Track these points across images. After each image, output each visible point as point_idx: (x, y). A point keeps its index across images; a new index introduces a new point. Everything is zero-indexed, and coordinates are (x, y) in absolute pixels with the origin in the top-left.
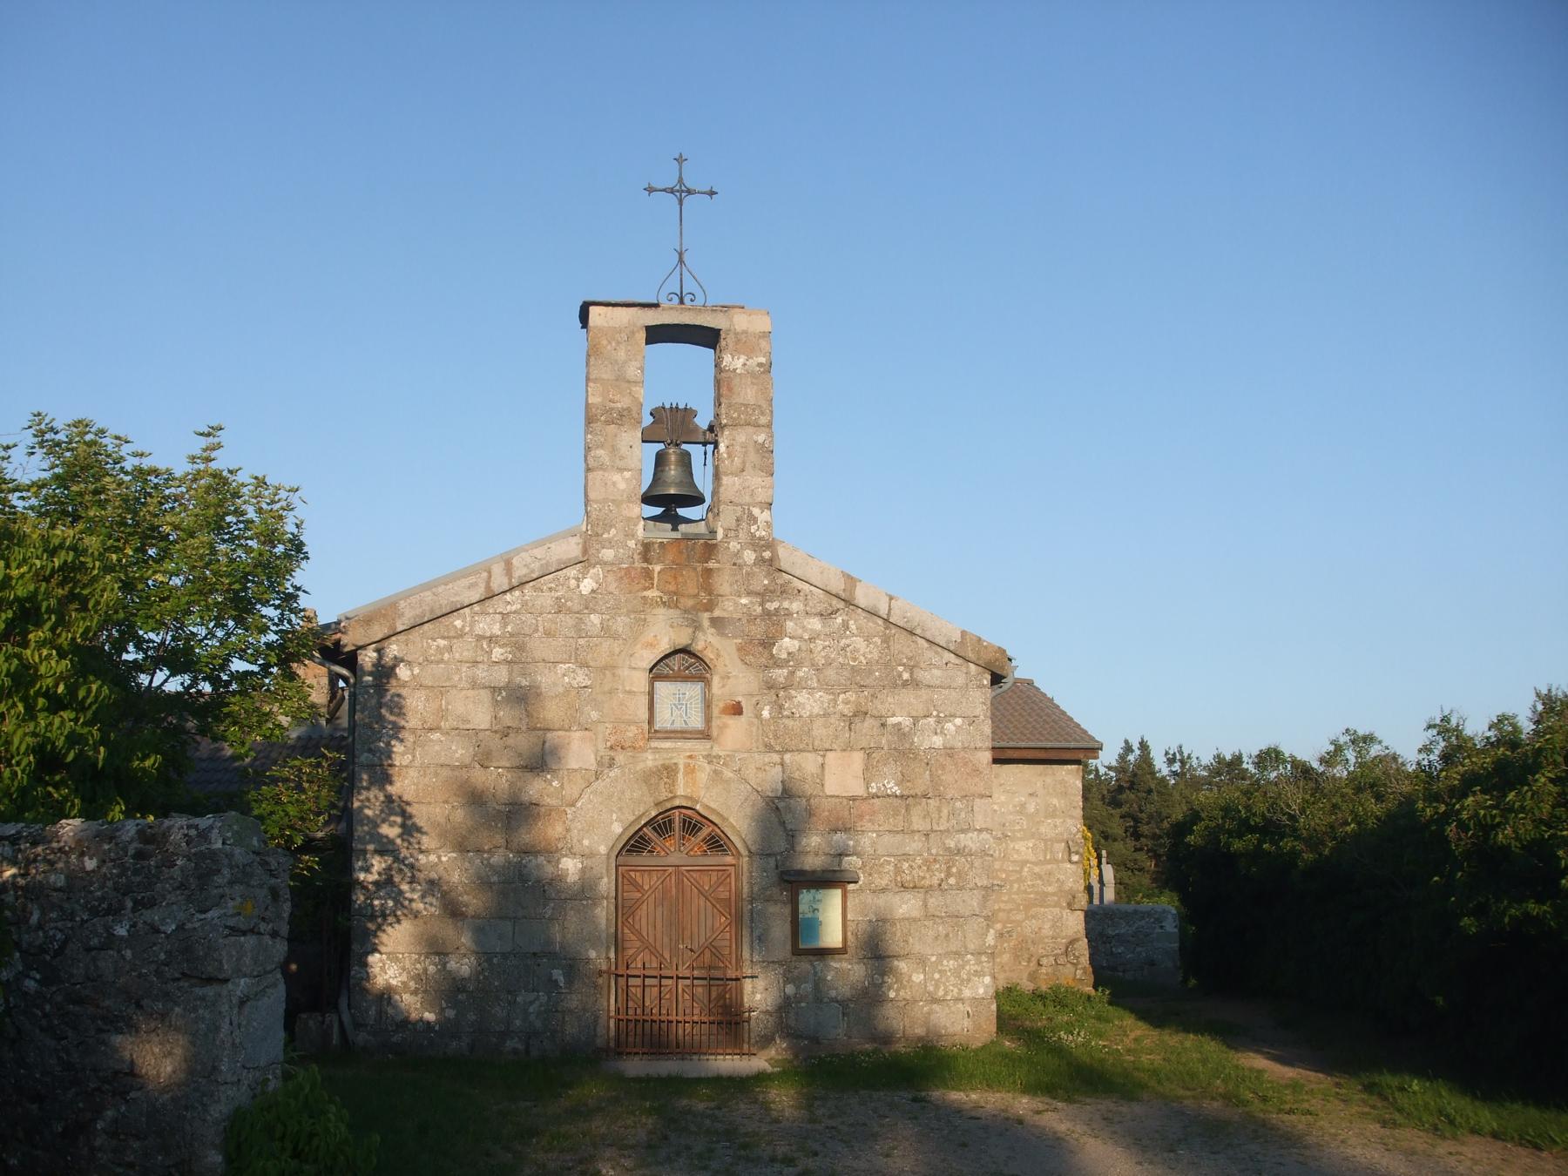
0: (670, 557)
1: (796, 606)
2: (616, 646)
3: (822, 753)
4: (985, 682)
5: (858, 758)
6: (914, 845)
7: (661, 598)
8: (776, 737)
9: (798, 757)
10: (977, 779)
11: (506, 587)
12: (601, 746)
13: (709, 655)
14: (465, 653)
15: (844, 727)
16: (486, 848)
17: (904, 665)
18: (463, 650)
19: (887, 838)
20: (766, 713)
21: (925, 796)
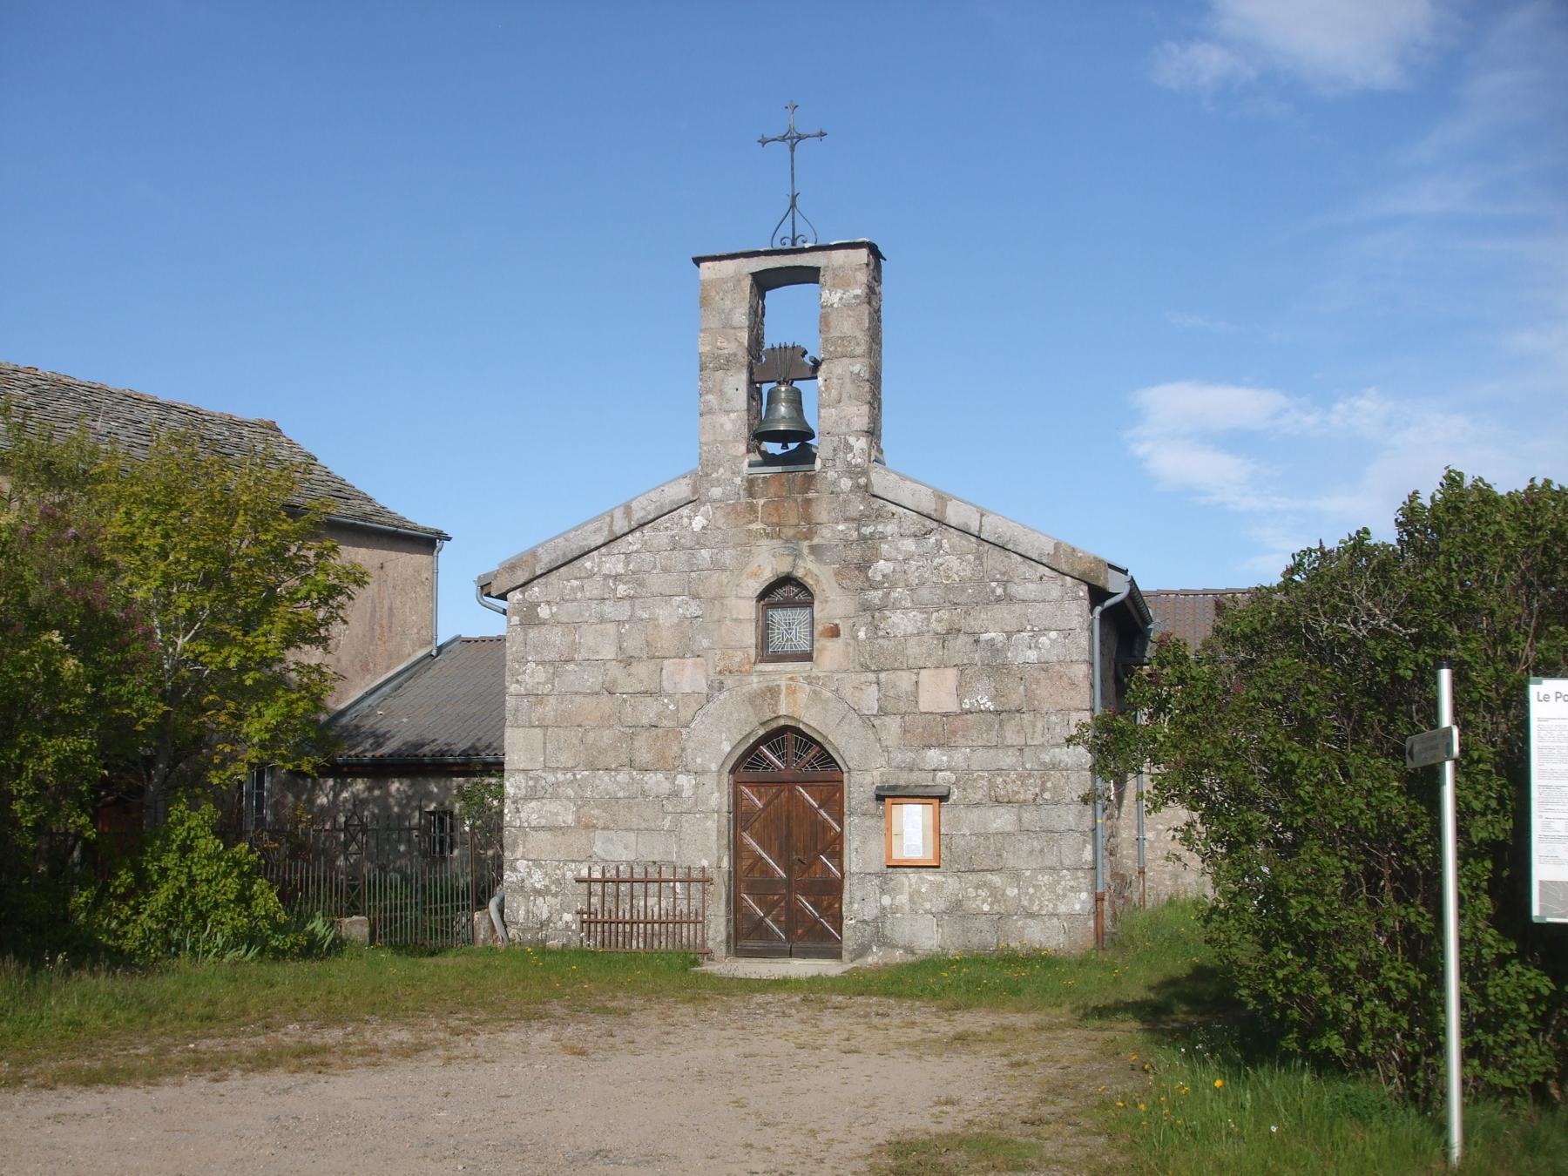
0: (772, 490)
1: (890, 528)
2: (724, 578)
3: (916, 671)
4: (1081, 594)
5: (951, 675)
6: (1008, 759)
7: (764, 529)
8: (872, 657)
9: (892, 676)
10: (1073, 693)
11: (626, 530)
12: (711, 672)
13: (810, 581)
14: (595, 592)
15: (938, 645)
16: (613, 766)
17: (997, 581)
18: (593, 588)
19: (980, 753)
20: (862, 635)
21: (1018, 711)
